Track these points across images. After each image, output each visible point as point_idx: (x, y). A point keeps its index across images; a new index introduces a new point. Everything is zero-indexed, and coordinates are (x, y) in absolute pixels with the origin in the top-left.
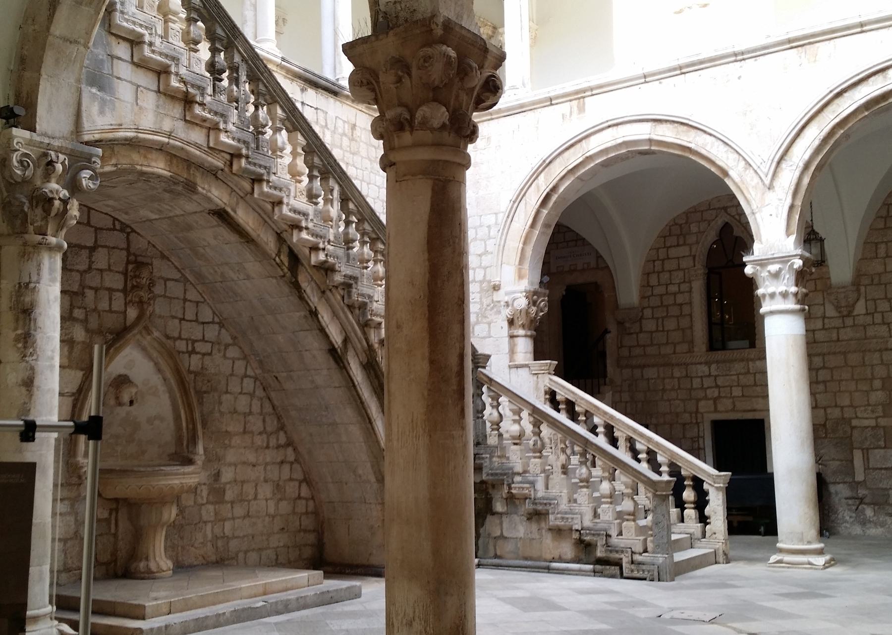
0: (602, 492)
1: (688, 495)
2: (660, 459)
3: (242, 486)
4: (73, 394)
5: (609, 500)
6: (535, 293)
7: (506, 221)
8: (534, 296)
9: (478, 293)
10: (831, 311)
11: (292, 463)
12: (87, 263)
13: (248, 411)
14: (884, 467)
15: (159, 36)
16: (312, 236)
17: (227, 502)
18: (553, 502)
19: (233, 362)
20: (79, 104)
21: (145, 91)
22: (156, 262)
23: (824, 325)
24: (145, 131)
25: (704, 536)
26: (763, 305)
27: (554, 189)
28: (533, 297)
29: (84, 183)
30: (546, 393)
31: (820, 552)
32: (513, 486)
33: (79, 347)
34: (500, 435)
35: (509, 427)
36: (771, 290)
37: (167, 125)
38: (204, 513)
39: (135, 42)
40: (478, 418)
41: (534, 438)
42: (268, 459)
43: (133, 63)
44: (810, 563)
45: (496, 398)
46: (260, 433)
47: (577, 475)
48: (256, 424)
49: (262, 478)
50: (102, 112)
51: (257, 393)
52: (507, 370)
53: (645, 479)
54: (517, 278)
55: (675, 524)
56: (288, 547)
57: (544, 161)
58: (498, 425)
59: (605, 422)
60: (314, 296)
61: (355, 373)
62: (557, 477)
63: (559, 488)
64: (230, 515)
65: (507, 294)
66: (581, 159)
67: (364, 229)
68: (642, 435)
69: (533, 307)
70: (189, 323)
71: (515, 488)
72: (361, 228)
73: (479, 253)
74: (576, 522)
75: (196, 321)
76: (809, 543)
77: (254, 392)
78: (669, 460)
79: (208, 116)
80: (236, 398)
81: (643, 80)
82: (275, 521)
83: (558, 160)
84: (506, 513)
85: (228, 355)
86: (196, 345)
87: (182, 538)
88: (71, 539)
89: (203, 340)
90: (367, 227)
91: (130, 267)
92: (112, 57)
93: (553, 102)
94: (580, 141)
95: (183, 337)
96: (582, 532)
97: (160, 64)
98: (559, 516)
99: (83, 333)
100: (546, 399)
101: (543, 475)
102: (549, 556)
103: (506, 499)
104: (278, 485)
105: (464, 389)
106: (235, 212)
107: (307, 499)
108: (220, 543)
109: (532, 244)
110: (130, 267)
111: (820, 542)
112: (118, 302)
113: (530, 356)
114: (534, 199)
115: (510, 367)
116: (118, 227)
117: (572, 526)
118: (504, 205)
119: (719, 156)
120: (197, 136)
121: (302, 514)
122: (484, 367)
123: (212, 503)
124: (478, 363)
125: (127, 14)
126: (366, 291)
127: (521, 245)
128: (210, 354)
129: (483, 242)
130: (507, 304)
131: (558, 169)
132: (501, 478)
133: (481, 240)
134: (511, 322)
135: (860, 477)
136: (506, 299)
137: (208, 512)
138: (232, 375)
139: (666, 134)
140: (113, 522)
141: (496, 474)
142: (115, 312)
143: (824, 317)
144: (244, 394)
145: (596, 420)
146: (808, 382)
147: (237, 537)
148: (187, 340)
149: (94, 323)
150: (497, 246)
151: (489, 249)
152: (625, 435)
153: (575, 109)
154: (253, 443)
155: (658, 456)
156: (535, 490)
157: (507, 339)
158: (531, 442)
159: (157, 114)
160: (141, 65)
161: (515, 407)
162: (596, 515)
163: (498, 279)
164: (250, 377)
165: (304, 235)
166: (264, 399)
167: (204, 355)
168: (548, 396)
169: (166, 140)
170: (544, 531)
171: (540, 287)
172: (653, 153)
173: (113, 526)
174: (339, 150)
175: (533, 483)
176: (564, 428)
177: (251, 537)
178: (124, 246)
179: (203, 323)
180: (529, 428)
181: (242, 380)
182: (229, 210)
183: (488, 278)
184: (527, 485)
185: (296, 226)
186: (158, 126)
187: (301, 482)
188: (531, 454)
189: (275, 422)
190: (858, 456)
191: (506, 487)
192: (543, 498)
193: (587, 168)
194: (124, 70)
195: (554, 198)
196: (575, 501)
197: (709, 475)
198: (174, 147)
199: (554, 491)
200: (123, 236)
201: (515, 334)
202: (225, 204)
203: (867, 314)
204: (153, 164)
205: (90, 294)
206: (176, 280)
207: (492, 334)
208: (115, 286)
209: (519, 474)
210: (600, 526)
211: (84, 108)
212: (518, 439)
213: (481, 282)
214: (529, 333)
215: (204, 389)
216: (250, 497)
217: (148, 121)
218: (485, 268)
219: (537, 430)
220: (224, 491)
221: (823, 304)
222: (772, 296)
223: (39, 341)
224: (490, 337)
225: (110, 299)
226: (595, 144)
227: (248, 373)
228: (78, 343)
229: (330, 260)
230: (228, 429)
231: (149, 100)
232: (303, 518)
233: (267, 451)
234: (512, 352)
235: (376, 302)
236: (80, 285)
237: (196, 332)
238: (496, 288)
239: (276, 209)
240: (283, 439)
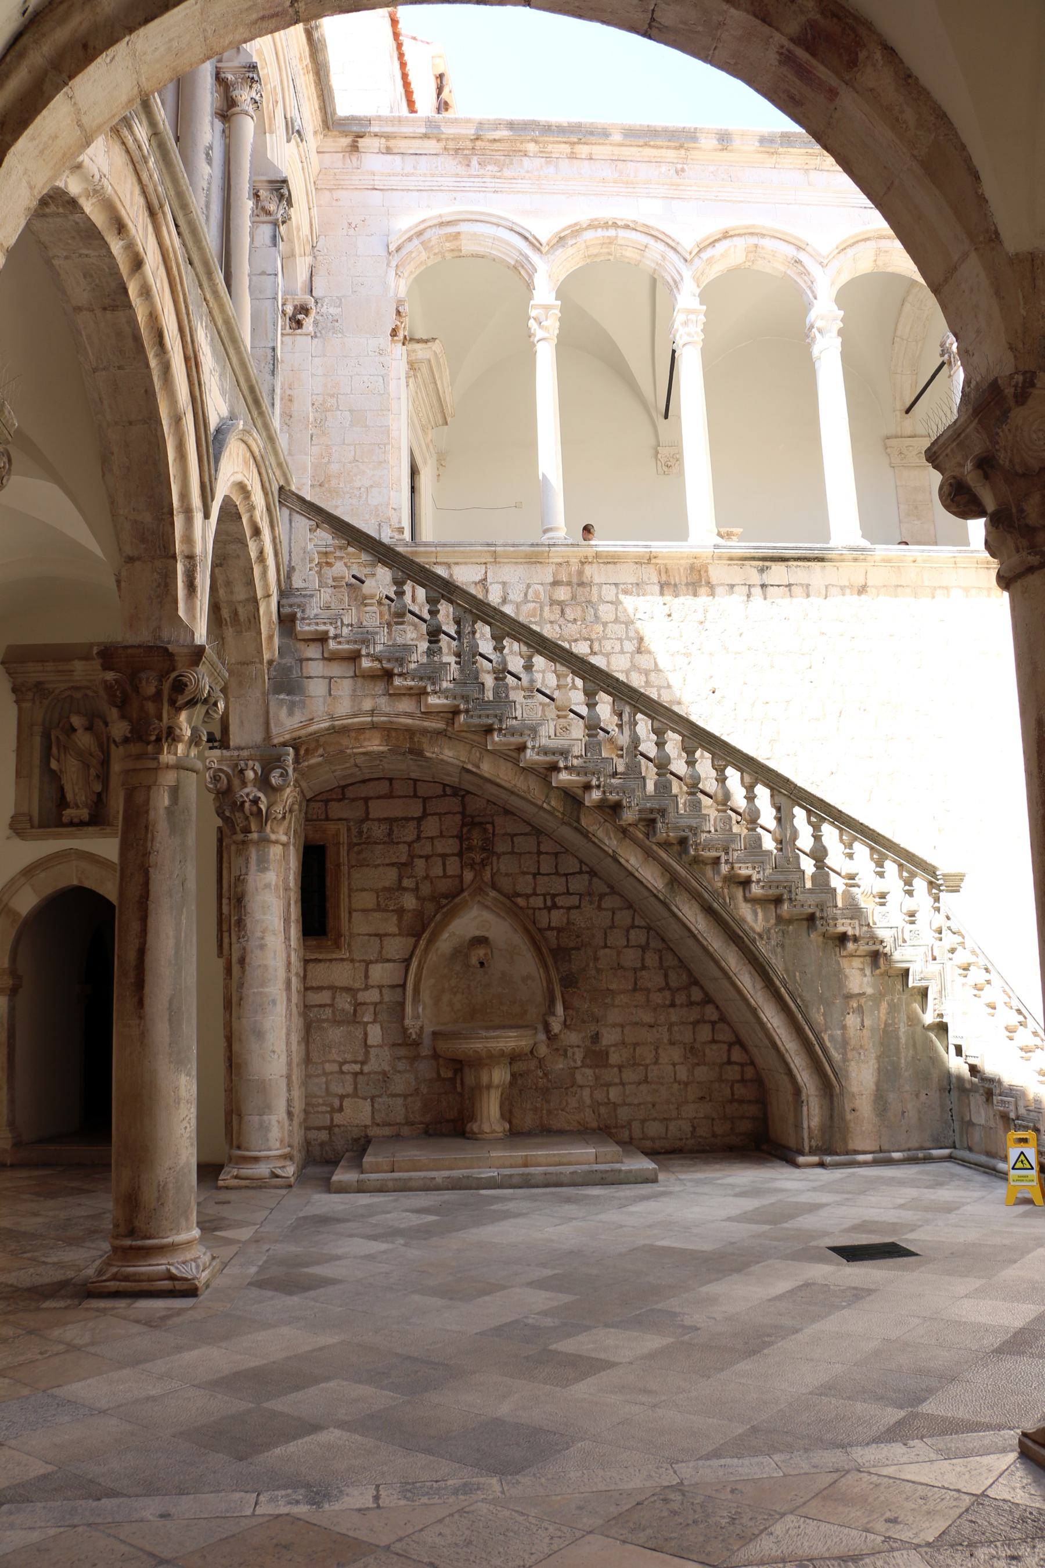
3: (635, 1049)
4: (405, 960)
11: (713, 1023)
12: (416, 833)
13: (639, 965)
15: (348, 625)
16: (578, 775)
17: (612, 1066)
19: (614, 913)
20: (267, 712)
21: (338, 680)
22: (499, 820)
24: (341, 718)
29: (273, 781)
33: (409, 914)
37: (367, 705)
38: (579, 1077)
39: (322, 639)
42: (674, 1019)
43: (324, 659)
46: (661, 990)
48: (653, 979)
49: (665, 1041)
50: (291, 713)
51: (652, 944)
56: (713, 1119)
60: (610, 838)
61: (693, 920)
64: (617, 1080)
70: (546, 878)
75: (557, 873)
77: (648, 943)
79: (412, 683)
80: (619, 953)
82: (689, 1089)
85: (604, 905)
86: (557, 899)
87: (548, 1102)
88: (411, 1095)
89: (568, 893)
91: (465, 830)
92: (301, 661)
95: (538, 892)
97: (352, 651)
99: (414, 901)
104: (692, 1048)
106: (478, 767)
107: (742, 1065)
108: (603, 1110)
110: (465, 830)
112: (453, 866)
116: (449, 791)
120: (406, 705)
121: (733, 1082)
123: (590, 1067)
125: (308, 618)
128: (579, 907)
137: (585, 1076)
138: (611, 928)
140: (458, 1081)
142: (450, 877)
144: (632, 947)
147: (630, 1105)
148: (544, 895)
149: (426, 889)
154: (648, 1000)
159: (354, 696)
160: (332, 658)
164: (639, 927)
165: (564, 776)
166: (664, 952)
167: (569, 908)
169: (369, 719)
173: (458, 1085)
177: (650, 1106)
178: (460, 809)
179: (566, 875)
181: (628, 931)
182: (470, 767)
185: (554, 768)
186: (356, 709)
187: (730, 1045)
189: (684, 976)
194: (315, 668)
198: (384, 722)
200: (456, 800)
202: (464, 762)
204: (366, 743)
205: (420, 863)
206: (526, 834)
208: (448, 851)
211: (271, 715)
215: (572, 945)
216: (648, 1062)
217: (344, 707)
220: (607, 1054)
223: (249, 925)
225: (444, 865)
227: (636, 923)
228: (409, 911)
229: (610, 797)
230: (610, 987)
231: (345, 688)
232: (736, 1086)
233: (672, 1010)
236: (409, 855)
237: (558, 885)
239: (522, 756)
240: (697, 995)
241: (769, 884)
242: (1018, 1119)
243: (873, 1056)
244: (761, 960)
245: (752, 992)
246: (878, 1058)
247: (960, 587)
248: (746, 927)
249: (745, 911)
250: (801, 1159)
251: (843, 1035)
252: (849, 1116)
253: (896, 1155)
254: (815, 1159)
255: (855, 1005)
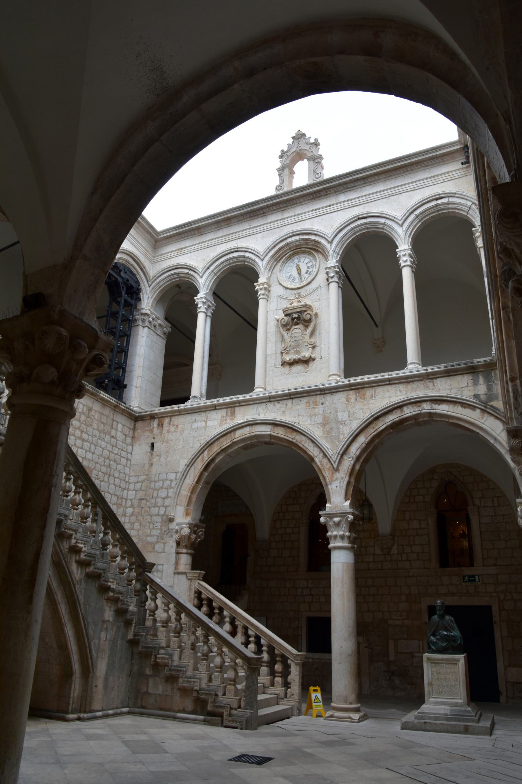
0: (215, 664)
1: (278, 667)
2: (263, 641)
5: (219, 670)
6: (196, 525)
7: (181, 478)
8: (195, 527)
9: (160, 522)
10: (378, 551)
14: (406, 651)
18: (183, 669)
23: (374, 558)
25: (286, 697)
26: (331, 542)
27: (213, 460)
28: (193, 528)
30: (195, 592)
31: (357, 710)
32: (158, 656)
34: (155, 621)
35: (161, 614)
36: (335, 533)
40: (142, 606)
41: (176, 623)
44: (350, 718)
45: (154, 594)
47: (201, 651)
52: (172, 575)
53: (243, 656)
54: (185, 515)
55: (268, 687)
57: (208, 442)
58: (154, 612)
59: (230, 614)
62: (188, 652)
63: (188, 660)
65: (178, 524)
66: (230, 443)
67: (69, 470)
68: (252, 625)
69: (193, 535)
71: (159, 658)
72: (67, 469)
73: (163, 496)
74: (196, 684)
76: (351, 703)
78: (268, 643)
81: (268, 400)
83: (216, 443)
84: (151, 676)
90: (71, 468)
93: (217, 408)
94: (230, 432)
96: (199, 692)
98: (185, 679)
100: (195, 596)
101: (178, 649)
102: (177, 709)
103: (153, 666)
105: (35, 579)
109: (197, 494)
111: (358, 703)
113: (189, 567)
114: (200, 465)
115: (175, 573)
117: (193, 687)
118: (181, 468)
119: (309, 448)
122: (150, 572)
124: (146, 568)
126: (62, 511)
127: (189, 494)
129: (166, 490)
130: (177, 532)
131: (216, 449)
132: (151, 650)
133: (165, 489)
134: (178, 544)
135: (392, 658)
136: (177, 527)
139: (280, 433)
141: (148, 647)
143: (374, 554)
145: (225, 613)
146: (355, 594)
150: (174, 493)
151: (170, 494)
152: (242, 624)
153: (229, 413)
155: (261, 639)
156: (172, 660)
157: (174, 555)
158: (173, 626)
161: (166, 601)
162: (210, 680)
163: (173, 515)
168: (196, 595)
170: (175, 690)
171: (200, 522)
172: (273, 444)
174: (77, 422)
175: (171, 656)
176: (195, 617)
180: (173, 616)
183: (167, 514)
184: (167, 656)
188: (173, 634)
190: (391, 643)
191: (153, 657)
192: (177, 666)
193: (233, 449)
195: (213, 466)
196: (198, 670)
197: (292, 654)
199: (185, 662)
201: (180, 551)
203: (398, 554)
207: (166, 551)
209: (163, 648)
210: (211, 688)
212: (166, 623)
213: (163, 516)
214: (189, 551)
218: (166, 507)
219: (178, 618)
221: (374, 546)
222: (335, 537)
224: (164, 552)
226: (239, 435)
234: (177, 563)
235: (71, 520)
238: (171, 520)
241: (88, 555)
242: (200, 690)
243: (107, 655)
244: (76, 597)
245: (64, 615)
246: (109, 656)
247: (122, 424)
248: (73, 577)
249: (74, 567)
250: (71, 716)
251: (99, 642)
252: (94, 690)
253: (111, 712)
254: (75, 716)
255: (105, 626)
